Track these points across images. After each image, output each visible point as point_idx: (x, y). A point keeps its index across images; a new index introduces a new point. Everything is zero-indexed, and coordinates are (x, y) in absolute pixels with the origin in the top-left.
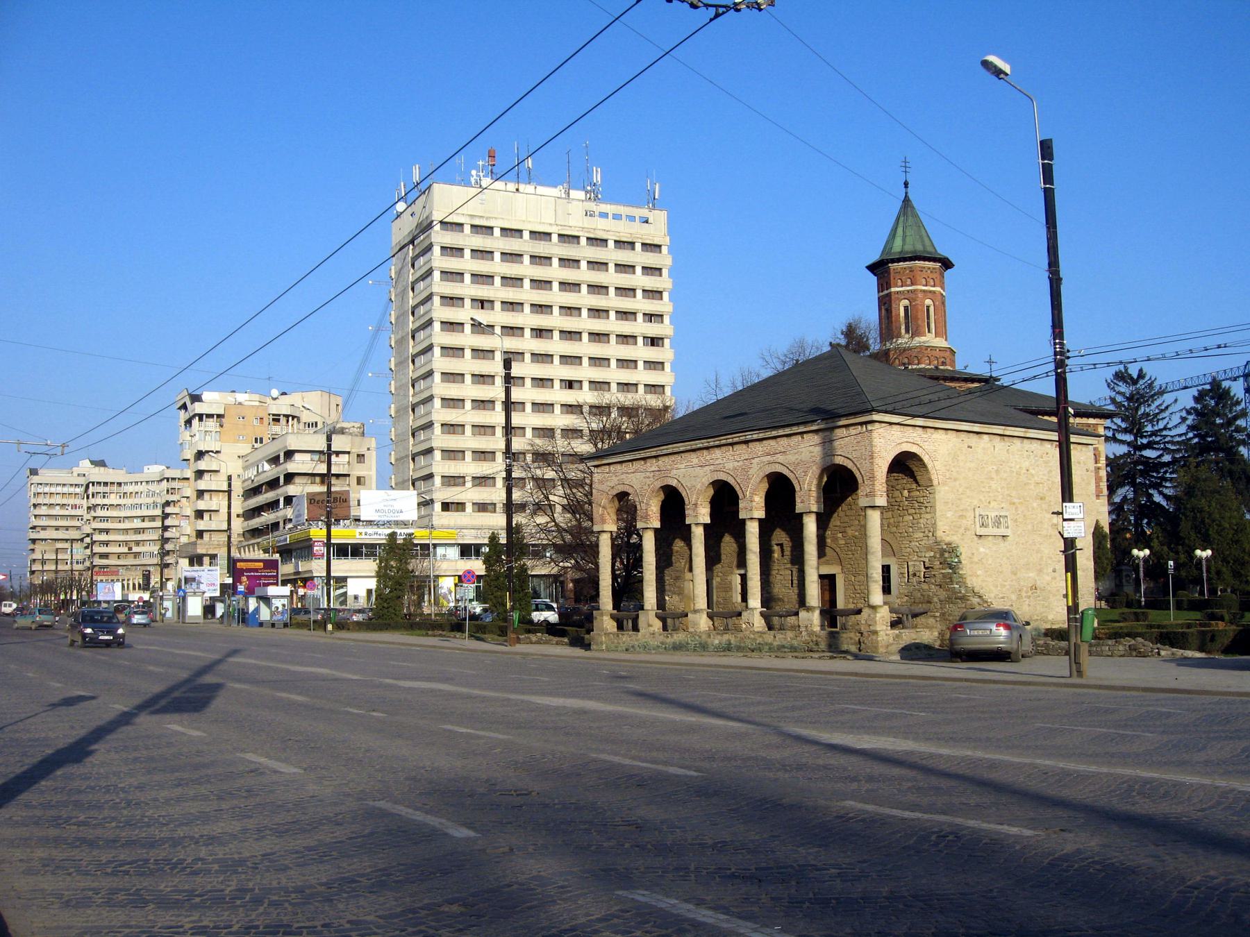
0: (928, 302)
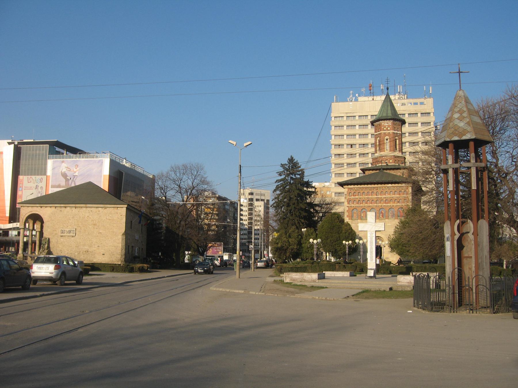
0: (387, 137)
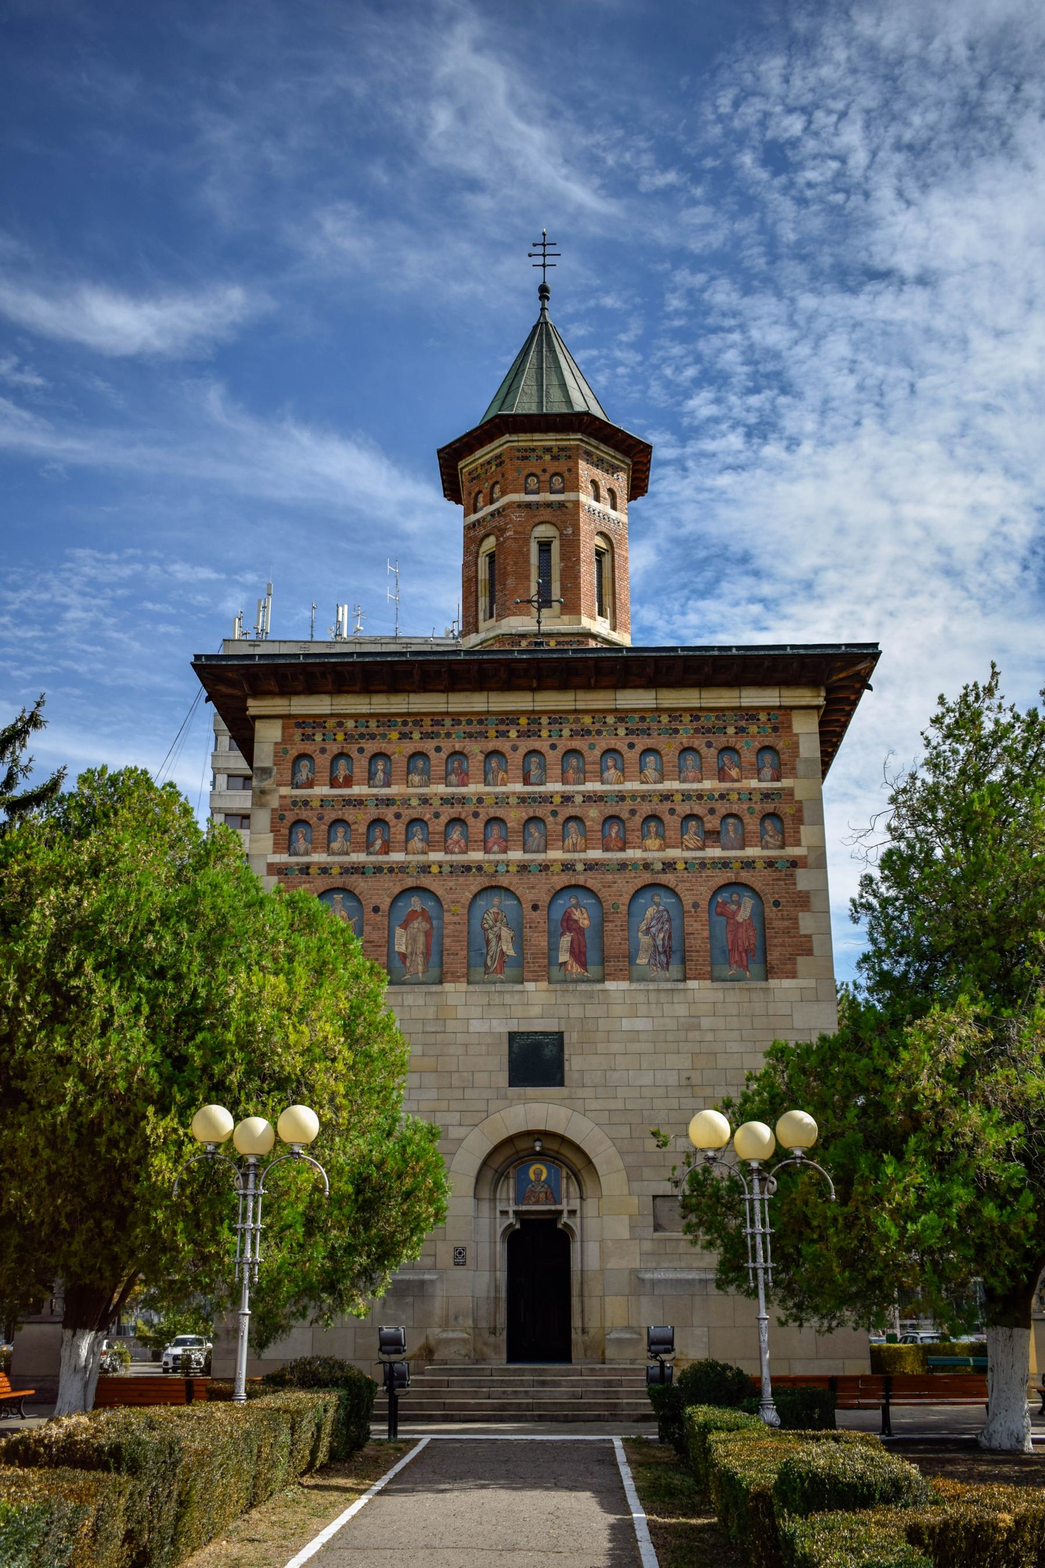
0: (543, 531)
